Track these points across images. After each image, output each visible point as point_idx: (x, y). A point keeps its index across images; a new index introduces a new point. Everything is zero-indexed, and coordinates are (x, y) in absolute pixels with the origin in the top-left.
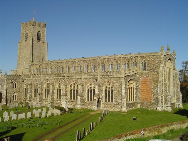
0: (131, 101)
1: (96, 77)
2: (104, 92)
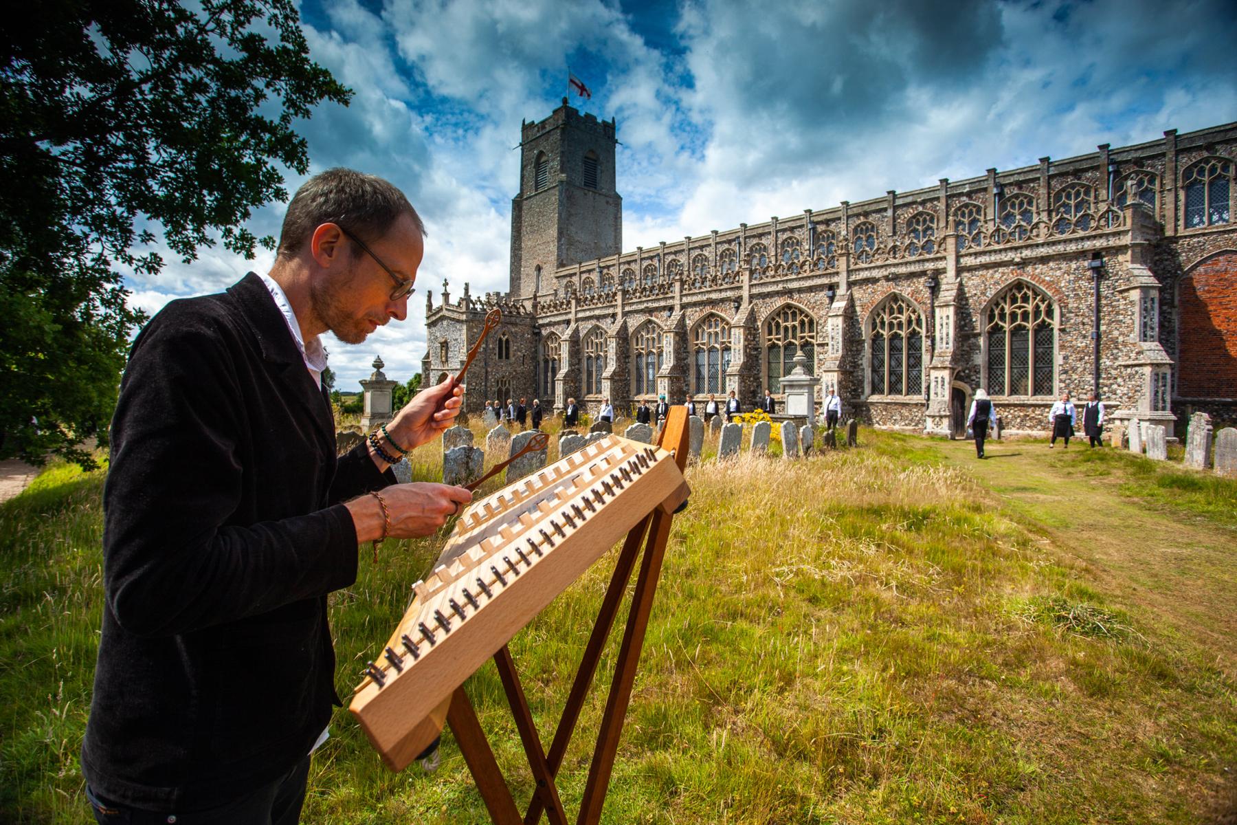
1: (930, 266)
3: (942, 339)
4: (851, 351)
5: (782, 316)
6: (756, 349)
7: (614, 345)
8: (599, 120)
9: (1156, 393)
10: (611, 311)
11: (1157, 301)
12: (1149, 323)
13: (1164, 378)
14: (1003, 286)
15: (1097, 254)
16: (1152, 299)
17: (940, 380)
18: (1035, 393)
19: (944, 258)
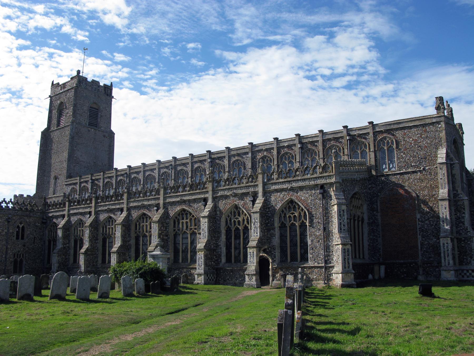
0: (359, 257)
1: (252, 190)
2: (277, 232)
3: (254, 231)
4: (215, 237)
5: (181, 216)
6: (167, 236)
7: (88, 231)
8: (102, 84)
9: (345, 259)
10: (88, 210)
11: (345, 211)
12: (342, 223)
13: (348, 251)
15: (322, 187)
16: (343, 210)
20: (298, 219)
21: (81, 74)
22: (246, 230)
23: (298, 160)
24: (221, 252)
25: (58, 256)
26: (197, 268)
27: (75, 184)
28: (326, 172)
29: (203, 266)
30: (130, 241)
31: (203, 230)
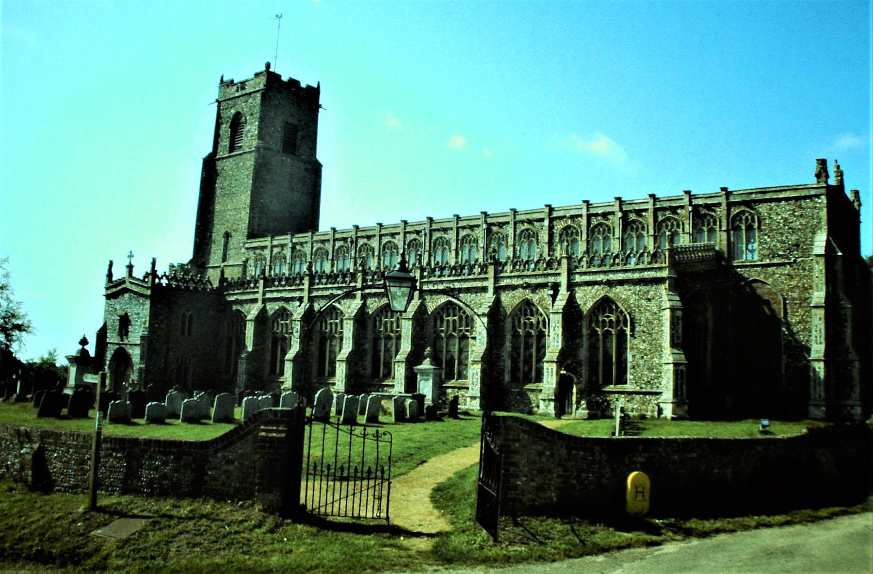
1: (551, 279)
2: (585, 342)
5: (445, 310)
7: (299, 327)
10: (297, 294)
14: (597, 299)
17: (550, 370)
18: (616, 384)
19: (559, 274)
20: (614, 325)
21: (272, 70)
22: (541, 335)
23: (617, 236)
24: (504, 367)
25: (247, 364)
26: (470, 389)
27: (263, 248)
28: (656, 262)
29: (479, 385)
30: (365, 345)
31: (480, 333)
